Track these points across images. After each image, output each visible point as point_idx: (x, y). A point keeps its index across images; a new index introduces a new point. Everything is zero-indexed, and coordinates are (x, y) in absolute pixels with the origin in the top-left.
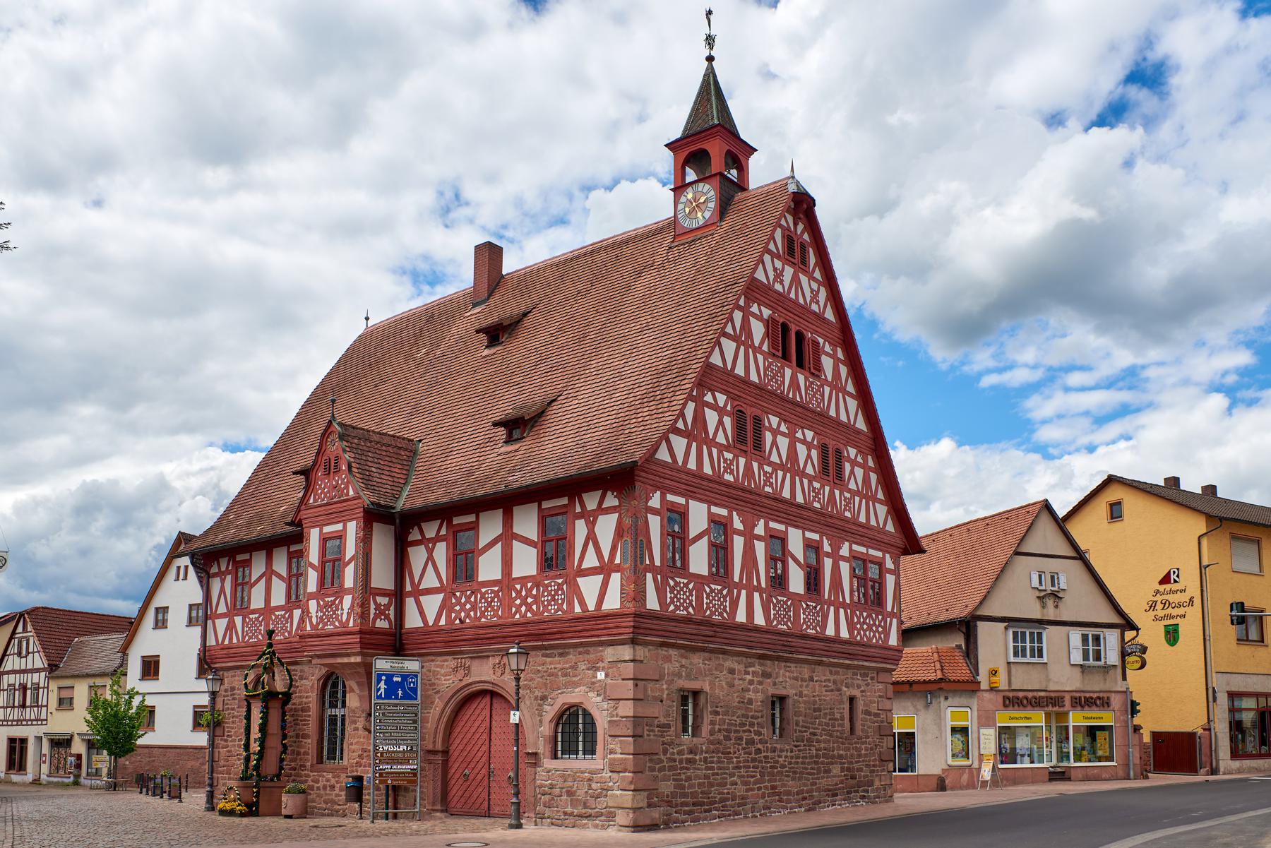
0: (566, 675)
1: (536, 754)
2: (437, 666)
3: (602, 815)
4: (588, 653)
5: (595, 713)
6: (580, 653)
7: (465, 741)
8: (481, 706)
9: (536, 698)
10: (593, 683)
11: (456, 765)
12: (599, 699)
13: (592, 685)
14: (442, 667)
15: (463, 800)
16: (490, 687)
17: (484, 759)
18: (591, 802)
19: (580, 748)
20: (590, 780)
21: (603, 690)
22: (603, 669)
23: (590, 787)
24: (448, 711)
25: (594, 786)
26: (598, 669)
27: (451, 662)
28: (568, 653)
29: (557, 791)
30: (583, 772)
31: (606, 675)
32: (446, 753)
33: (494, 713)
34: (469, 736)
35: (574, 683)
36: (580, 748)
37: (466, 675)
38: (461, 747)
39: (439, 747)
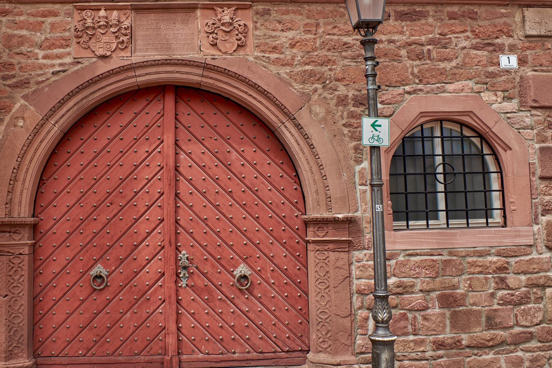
0: (419, 57)
1: (350, 222)
2: (20, 26)
3: (530, 337)
4: (473, 17)
5: (502, 130)
6: (452, 16)
7: (93, 200)
8: (144, 120)
9: (342, 101)
10: (492, 75)
11: (62, 257)
12: (513, 105)
13: (491, 79)
14: (37, 27)
15: (87, 336)
16: (193, 76)
17: (155, 240)
18: (508, 315)
19: (442, 205)
20: (503, 269)
21: (516, 89)
22: (512, 49)
23: (502, 283)
24: (53, 131)
25: (512, 279)
26: (501, 49)
27: (68, 19)
28: (423, 15)
29: (417, 298)
30: (481, 254)
31: (522, 62)
32: (35, 227)
33: (183, 134)
34: (104, 187)
35: (443, 72)
36: (442, 205)
37: (122, 46)
38: (78, 213)
39: (22, 212)
